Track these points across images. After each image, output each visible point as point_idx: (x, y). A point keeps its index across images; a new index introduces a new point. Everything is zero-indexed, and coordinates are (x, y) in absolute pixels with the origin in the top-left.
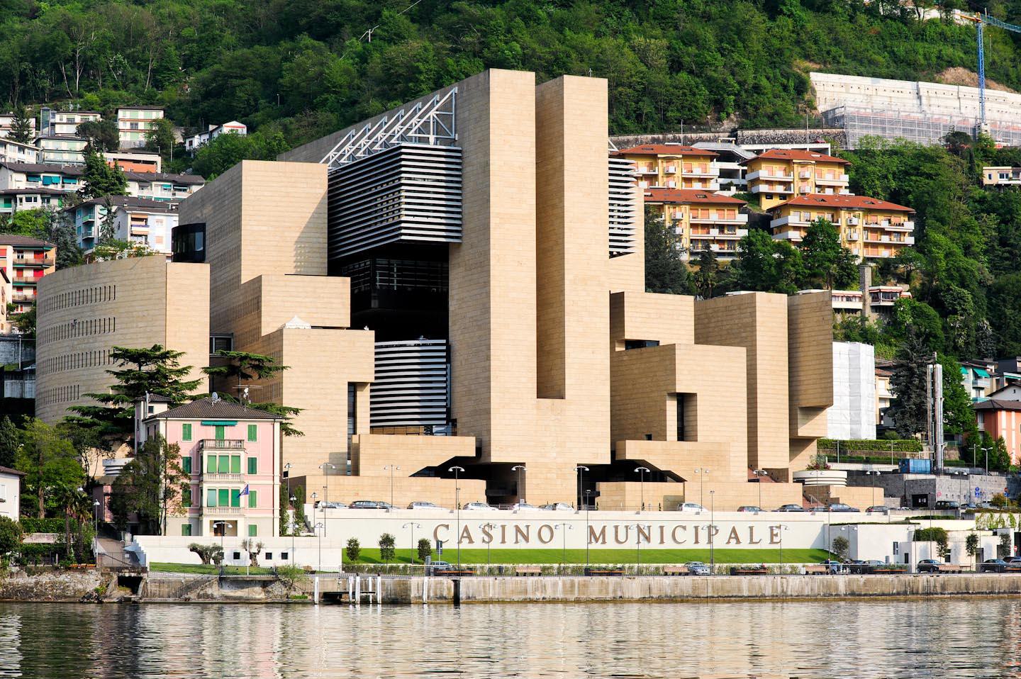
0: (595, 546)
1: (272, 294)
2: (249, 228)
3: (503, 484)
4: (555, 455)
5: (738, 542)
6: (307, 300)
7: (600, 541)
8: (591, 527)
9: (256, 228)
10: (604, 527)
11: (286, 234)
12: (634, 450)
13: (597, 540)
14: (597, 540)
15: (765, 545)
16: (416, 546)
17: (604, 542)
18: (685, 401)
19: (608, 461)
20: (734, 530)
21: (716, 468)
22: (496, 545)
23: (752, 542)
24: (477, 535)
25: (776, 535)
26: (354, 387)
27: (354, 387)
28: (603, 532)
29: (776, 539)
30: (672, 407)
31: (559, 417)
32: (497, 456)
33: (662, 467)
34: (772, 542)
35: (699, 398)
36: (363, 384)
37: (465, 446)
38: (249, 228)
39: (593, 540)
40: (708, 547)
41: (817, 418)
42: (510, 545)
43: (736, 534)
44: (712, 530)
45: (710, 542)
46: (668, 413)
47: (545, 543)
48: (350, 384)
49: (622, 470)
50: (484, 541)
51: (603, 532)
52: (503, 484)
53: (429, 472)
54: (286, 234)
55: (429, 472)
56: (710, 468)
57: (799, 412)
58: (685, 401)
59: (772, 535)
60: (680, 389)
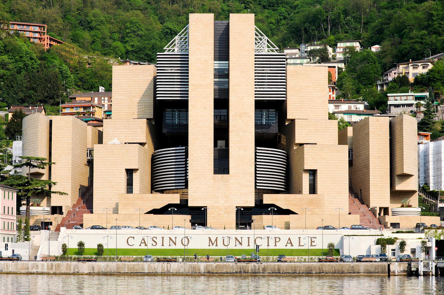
0: (213, 247)
1: (108, 128)
2: (115, 97)
3: (199, 216)
4: (223, 202)
5: (292, 245)
6: (125, 130)
7: (215, 244)
8: (210, 238)
9: (119, 97)
10: (217, 238)
11: (133, 99)
13: (213, 244)
14: (213, 244)
15: (306, 247)
16: (96, 247)
17: (217, 245)
18: (313, 173)
19: (251, 203)
20: (289, 239)
21: (316, 207)
22: (159, 246)
23: (300, 245)
24: (150, 243)
27: (130, 172)
28: (216, 240)
29: (313, 244)
31: (226, 183)
32: (191, 203)
33: (284, 207)
34: (311, 245)
37: (175, 199)
38: (115, 97)
39: (211, 244)
40: (266, 248)
41: (408, 180)
42: (166, 247)
43: (290, 241)
44: (277, 240)
45: (276, 245)
46: (304, 180)
47: (185, 246)
48: (127, 170)
49: (261, 208)
50: (152, 245)
51: (216, 240)
52: (199, 216)
53: (155, 212)
54: (133, 99)
55: (155, 212)
56: (312, 207)
57: (396, 177)
59: (312, 242)
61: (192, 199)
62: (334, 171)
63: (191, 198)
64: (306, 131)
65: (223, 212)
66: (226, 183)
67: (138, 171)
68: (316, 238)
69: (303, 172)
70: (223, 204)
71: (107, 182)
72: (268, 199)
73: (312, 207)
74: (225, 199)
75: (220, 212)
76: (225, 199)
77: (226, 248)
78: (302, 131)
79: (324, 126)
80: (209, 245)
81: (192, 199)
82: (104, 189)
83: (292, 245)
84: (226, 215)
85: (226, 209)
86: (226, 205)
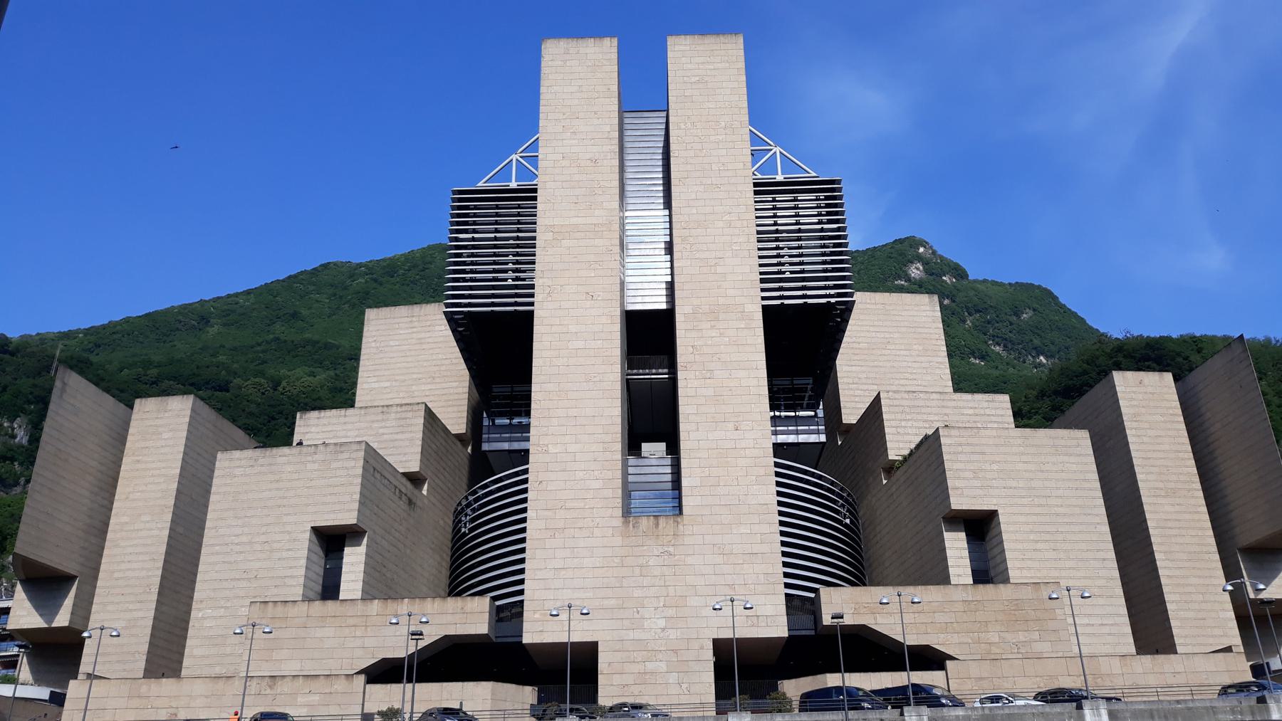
2: (365, 386)
4: (662, 623)
9: (376, 385)
12: (843, 605)
18: (980, 526)
26: (332, 541)
27: (332, 541)
30: (956, 545)
31: (671, 549)
32: (536, 631)
35: (1002, 518)
37: (470, 617)
38: (365, 386)
48: (319, 532)
56: (1022, 636)
58: (980, 526)
60: (960, 501)
61: (537, 616)
62: (1058, 515)
64: (915, 424)
65: (663, 667)
66: (671, 549)
70: (663, 629)
71: (245, 576)
73: (1022, 636)
74: (671, 612)
75: (650, 666)
76: (671, 612)
78: (903, 424)
79: (971, 412)
81: (537, 616)
82: (229, 605)
84: (673, 678)
86: (673, 634)
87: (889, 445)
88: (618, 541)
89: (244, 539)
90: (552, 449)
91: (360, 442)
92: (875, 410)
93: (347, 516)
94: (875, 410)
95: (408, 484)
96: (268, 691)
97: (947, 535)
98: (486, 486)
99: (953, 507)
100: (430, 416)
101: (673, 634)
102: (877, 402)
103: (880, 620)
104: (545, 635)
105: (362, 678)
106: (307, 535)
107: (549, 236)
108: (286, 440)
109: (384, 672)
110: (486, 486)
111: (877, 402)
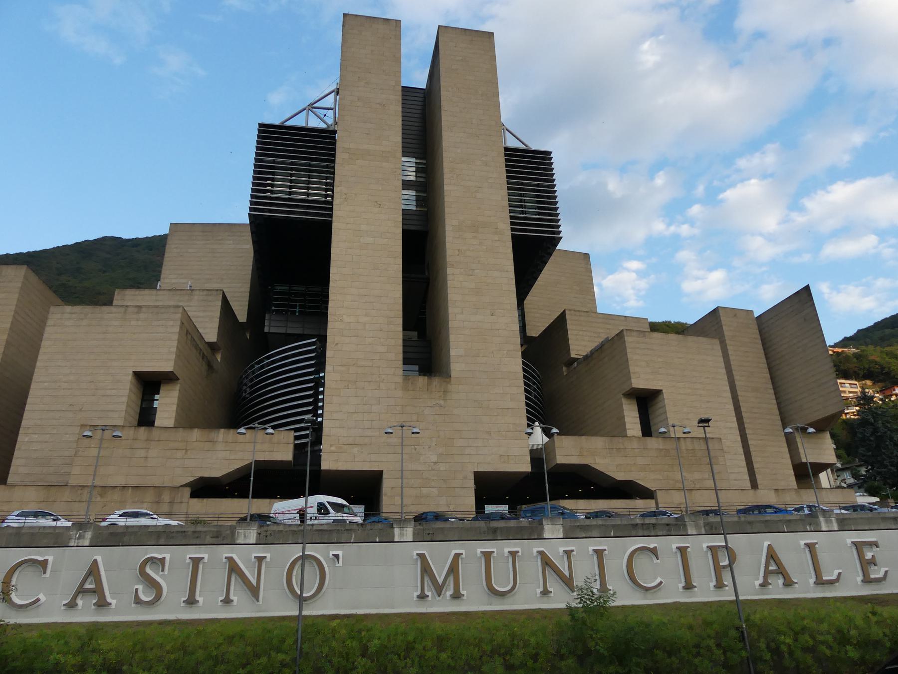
4: (434, 458)
5: (788, 583)
10: (457, 556)
13: (439, 589)
14: (439, 589)
17: (457, 596)
18: (646, 401)
23: (820, 582)
25: (873, 562)
26: (149, 384)
27: (149, 384)
28: (453, 570)
29: (877, 573)
32: (332, 459)
34: (867, 580)
35: (666, 395)
36: (167, 378)
37: (277, 446)
43: (778, 563)
50: (138, 601)
51: (453, 570)
58: (646, 401)
59: (866, 565)
60: (640, 382)
61: (333, 448)
63: (331, 445)
65: (435, 491)
67: (178, 387)
68: (875, 544)
69: (624, 401)
70: (435, 463)
72: (569, 451)
74: (441, 450)
75: (425, 491)
76: (441, 450)
77: (497, 606)
78: (581, 333)
80: (422, 597)
81: (333, 448)
83: (788, 583)
85: (444, 480)
86: (442, 467)
87: (571, 347)
88: (400, 393)
89: (72, 378)
90: (346, 319)
91: (178, 307)
92: (561, 321)
93: (166, 365)
94: (561, 321)
95: (209, 350)
96: (99, 499)
97: (624, 406)
98: (272, 356)
99: (634, 386)
100: (226, 303)
101: (442, 467)
102: (563, 316)
103: (598, 460)
104: (340, 464)
105: (187, 491)
106: (130, 378)
107: (346, 156)
108: (109, 303)
109: (205, 488)
110: (272, 356)
111: (563, 316)
